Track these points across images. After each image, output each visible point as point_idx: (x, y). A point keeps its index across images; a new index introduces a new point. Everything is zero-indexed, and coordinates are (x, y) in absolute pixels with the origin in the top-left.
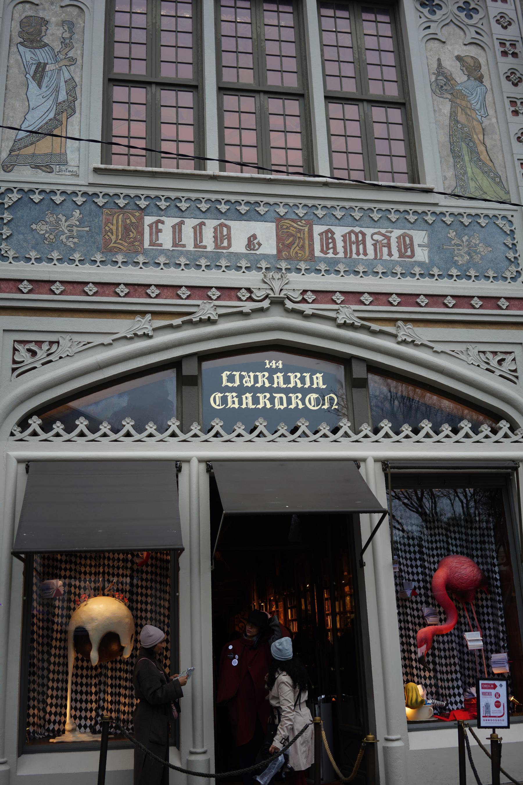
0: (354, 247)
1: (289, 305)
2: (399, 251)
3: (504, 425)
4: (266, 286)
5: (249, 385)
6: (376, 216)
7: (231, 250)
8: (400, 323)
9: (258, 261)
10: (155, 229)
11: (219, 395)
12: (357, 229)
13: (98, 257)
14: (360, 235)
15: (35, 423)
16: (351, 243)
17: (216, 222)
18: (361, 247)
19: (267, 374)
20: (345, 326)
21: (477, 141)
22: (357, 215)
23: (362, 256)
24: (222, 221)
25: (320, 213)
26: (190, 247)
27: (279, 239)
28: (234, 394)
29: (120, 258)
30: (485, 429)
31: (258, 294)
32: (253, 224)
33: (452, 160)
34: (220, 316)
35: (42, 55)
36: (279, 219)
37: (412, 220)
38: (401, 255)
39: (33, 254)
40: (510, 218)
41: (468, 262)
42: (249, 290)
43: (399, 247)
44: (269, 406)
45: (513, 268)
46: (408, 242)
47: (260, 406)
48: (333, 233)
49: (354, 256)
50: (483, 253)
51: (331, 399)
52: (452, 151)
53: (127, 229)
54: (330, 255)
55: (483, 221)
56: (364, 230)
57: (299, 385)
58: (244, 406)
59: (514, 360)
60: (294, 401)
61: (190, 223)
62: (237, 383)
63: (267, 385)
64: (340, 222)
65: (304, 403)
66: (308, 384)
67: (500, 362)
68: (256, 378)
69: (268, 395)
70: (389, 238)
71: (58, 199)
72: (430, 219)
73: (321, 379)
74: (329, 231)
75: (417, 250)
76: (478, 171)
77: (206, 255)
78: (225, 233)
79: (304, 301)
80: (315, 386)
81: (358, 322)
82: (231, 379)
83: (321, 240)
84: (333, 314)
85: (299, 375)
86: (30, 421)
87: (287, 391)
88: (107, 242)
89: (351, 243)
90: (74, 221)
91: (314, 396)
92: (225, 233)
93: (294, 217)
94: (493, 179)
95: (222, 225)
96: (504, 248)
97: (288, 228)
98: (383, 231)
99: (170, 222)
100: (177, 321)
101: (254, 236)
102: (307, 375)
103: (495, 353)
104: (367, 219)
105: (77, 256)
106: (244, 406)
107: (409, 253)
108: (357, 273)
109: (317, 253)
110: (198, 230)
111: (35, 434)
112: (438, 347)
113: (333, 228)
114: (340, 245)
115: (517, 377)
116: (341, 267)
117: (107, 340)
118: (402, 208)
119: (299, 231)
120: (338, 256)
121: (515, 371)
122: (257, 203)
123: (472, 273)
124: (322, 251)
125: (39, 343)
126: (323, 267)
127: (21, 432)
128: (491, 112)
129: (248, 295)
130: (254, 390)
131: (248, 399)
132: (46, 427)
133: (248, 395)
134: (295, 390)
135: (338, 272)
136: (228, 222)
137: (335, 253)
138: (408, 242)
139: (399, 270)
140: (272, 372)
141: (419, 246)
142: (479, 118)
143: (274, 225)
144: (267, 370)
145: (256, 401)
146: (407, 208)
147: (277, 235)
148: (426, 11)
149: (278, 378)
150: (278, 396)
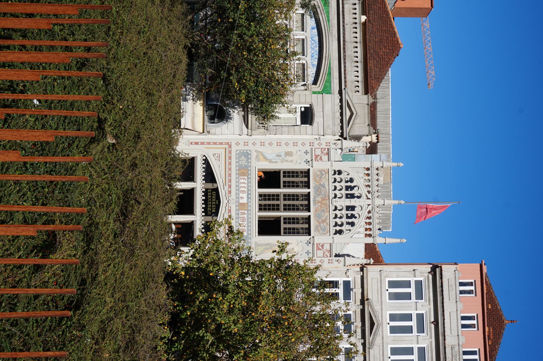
1: (228, 204)
10: (244, 179)
13: (237, 168)
15: (204, 158)
25: (249, 212)
26: (240, 185)
27: (243, 203)
29: (237, 172)
33: (265, 243)
35: (283, 156)
36: (247, 203)
39: (237, 156)
52: (267, 244)
53: (244, 173)
61: (246, 186)
64: (247, 217)
71: (249, 160)
76: (262, 249)
77: (239, 188)
82: (214, 194)
87: (211, 204)
88: (240, 170)
90: (245, 163)
99: (246, 182)
100: (224, 182)
105: (237, 164)
109: (240, 211)
110: (244, 187)
114: (243, 216)
125: (219, 158)
130: (212, 198)
131: (210, 197)
132: (203, 160)
134: (212, 206)
140: (216, 202)
143: (246, 202)
145: (209, 198)
148: (306, 242)
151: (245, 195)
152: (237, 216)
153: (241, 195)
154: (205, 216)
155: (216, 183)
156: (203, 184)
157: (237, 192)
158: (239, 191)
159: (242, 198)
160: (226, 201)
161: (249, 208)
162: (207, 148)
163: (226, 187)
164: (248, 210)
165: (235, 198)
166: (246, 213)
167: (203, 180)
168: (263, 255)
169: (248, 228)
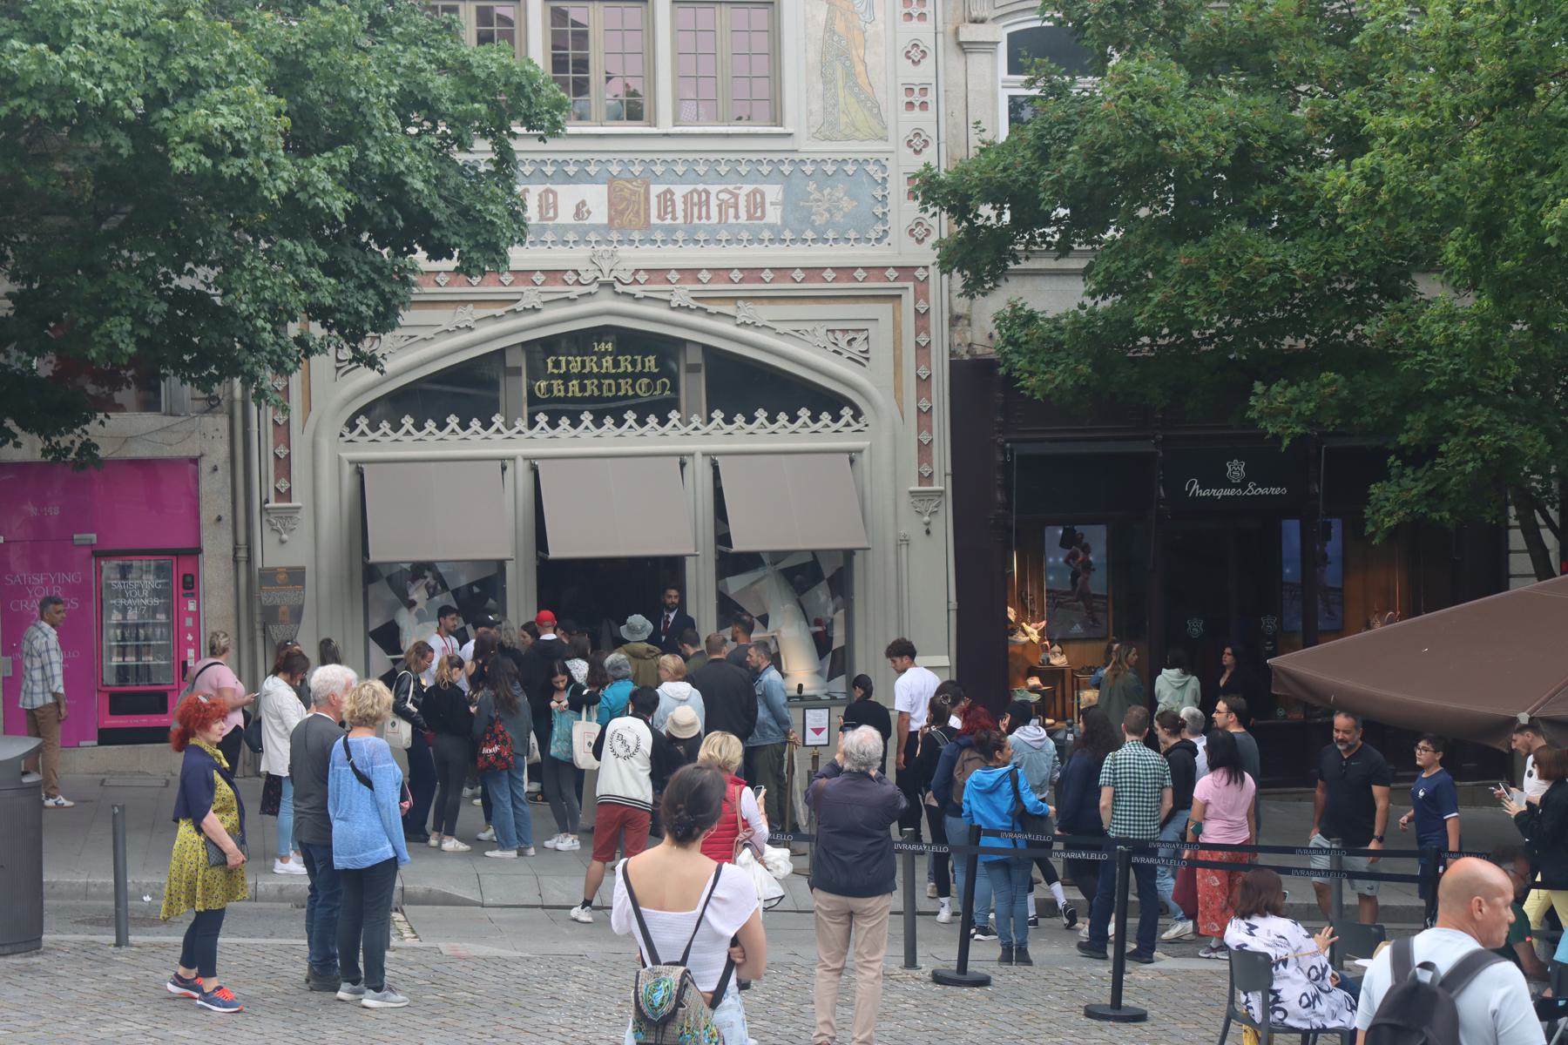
0: (696, 209)
1: (619, 288)
2: (748, 211)
3: (847, 413)
4: (594, 267)
5: (576, 371)
6: (723, 169)
7: (559, 221)
8: (740, 303)
9: (587, 233)
11: (543, 384)
12: (700, 187)
14: (704, 195)
15: (362, 422)
16: (693, 204)
17: (542, 188)
18: (704, 209)
19: (595, 358)
20: (680, 308)
21: (856, 59)
22: (701, 169)
23: (704, 221)
24: (548, 185)
25: (659, 169)
27: (611, 204)
28: (560, 382)
30: (825, 417)
31: (586, 277)
32: (582, 187)
33: (820, 87)
34: (544, 302)
36: (611, 180)
37: (765, 173)
38: (750, 217)
40: (884, 162)
41: (828, 222)
42: (576, 272)
43: (748, 207)
44: (596, 393)
45: (880, 227)
46: (759, 199)
47: (587, 394)
48: (672, 194)
49: (696, 221)
50: (846, 210)
51: (664, 385)
54: (668, 221)
55: (850, 169)
56: (708, 187)
57: (630, 369)
58: (570, 394)
59: (867, 339)
60: (623, 387)
62: (564, 369)
63: (595, 370)
64: (681, 179)
65: (634, 389)
66: (639, 367)
67: (850, 342)
68: (583, 362)
69: (596, 382)
70: (736, 197)
72: (786, 169)
73: (653, 362)
74: (669, 191)
75: (769, 209)
78: (551, 200)
79: (636, 282)
80: (646, 370)
81: (693, 305)
82: (557, 365)
83: (659, 202)
84: (666, 296)
85: (629, 358)
86: (357, 422)
87: (616, 377)
89: (693, 204)
91: (645, 381)
92: (551, 200)
93: (629, 175)
94: (871, 110)
95: (547, 191)
96: (872, 201)
97: (621, 190)
98: (730, 187)
100: (499, 311)
101: (583, 203)
102: (639, 358)
103: (845, 331)
104: (713, 174)
106: (570, 394)
107: (759, 214)
108: (697, 242)
109: (654, 220)
111: (363, 433)
112: (781, 328)
113: (673, 188)
114: (680, 207)
115: (867, 359)
116: (680, 236)
117: (428, 333)
118: (754, 157)
119: (634, 193)
120: (677, 222)
121: (866, 352)
122: (588, 162)
123: (831, 235)
124: (659, 217)
126: (659, 236)
127: (351, 432)
128: (879, 15)
129: (575, 278)
130: (581, 377)
132: (374, 427)
133: (575, 382)
134: (625, 375)
135: (675, 242)
136: (553, 187)
137: (674, 218)
138: (759, 199)
139: (745, 236)
140: (603, 355)
141: (772, 204)
142: (862, 24)
144: (595, 353)
145: (583, 388)
146: (761, 156)
147: (609, 201)
149: (608, 362)
150: (607, 382)
151: (568, 196)
152: (680, 236)
153: (566, 216)
154: (679, 411)
155: (501, 352)
156: (509, 425)
157: (549, 237)
158: (544, 229)
159: (581, 210)
160: (606, 302)
161: (637, 170)
162: (308, 407)
163: (530, 297)
164: (649, 178)
165: (583, 252)
166: (662, 188)
167: (487, 425)
168: (880, 96)
169: (744, 178)
